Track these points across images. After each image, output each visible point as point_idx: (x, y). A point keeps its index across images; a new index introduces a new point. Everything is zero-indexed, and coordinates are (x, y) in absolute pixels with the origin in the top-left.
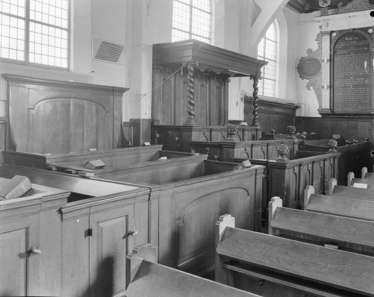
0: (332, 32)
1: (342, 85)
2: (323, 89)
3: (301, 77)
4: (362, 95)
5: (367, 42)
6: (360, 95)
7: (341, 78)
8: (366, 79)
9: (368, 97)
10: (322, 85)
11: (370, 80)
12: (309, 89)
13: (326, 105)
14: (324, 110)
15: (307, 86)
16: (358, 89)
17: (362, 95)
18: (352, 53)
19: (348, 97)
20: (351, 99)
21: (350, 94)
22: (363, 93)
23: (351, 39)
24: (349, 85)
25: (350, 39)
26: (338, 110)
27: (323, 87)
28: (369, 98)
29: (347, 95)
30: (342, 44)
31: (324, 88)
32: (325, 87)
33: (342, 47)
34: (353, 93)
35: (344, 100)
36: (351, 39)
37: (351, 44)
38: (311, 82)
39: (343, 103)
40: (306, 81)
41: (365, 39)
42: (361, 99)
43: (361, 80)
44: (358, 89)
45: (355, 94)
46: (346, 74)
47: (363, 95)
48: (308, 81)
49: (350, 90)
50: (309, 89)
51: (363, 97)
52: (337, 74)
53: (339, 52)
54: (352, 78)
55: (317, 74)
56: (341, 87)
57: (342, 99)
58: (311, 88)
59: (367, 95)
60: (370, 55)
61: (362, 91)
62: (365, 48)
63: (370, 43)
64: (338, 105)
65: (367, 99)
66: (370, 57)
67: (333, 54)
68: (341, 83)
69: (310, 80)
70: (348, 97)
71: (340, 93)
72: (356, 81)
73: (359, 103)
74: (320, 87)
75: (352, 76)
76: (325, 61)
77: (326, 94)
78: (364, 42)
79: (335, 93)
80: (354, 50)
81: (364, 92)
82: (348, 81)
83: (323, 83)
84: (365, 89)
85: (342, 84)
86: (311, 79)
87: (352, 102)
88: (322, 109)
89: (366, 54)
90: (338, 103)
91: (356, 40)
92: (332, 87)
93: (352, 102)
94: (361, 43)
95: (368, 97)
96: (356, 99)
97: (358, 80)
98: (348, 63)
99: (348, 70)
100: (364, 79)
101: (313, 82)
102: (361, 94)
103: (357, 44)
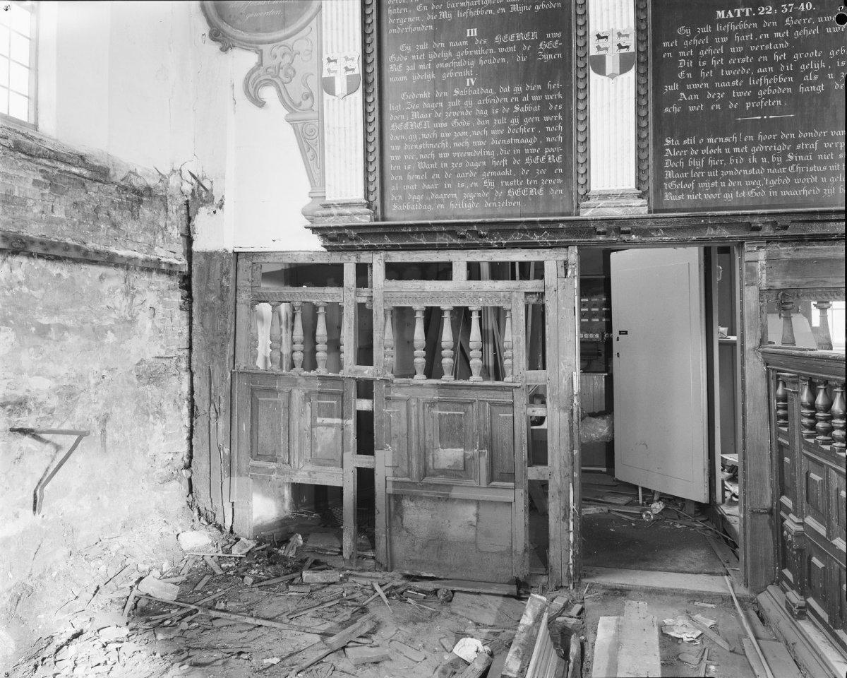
1: (421, 72)
2: (326, 96)
3: (216, 35)
4: (526, 121)
6: (515, 121)
7: (418, 38)
8: (542, 37)
9: (554, 134)
10: (325, 74)
11: (567, 40)
12: (260, 103)
13: (346, 184)
14: (334, 211)
15: (247, 79)
16: (508, 89)
19: (457, 135)
20: (471, 149)
21: (467, 118)
22: (530, 114)
24: (457, 69)
26: (405, 209)
27: (328, 86)
28: (560, 138)
29: (450, 129)
31: (332, 92)
32: (340, 85)
34: (479, 112)
35: (437, 151)
38: (268, 61)
39: (432, 171)
40: (243, 60)
42: (522, 147)
43: (519, 44)
44: (508, 89)
45: (490, 117)
46: (444, 15)
47: (530, 125)
48: (251, 59)
49: (464, 98)
50: (260, 103)
51: (529, 135)
52: (395, 16)
54: (472, 32)
55: (300, 16)
56: (421, 86)
57: (423, 151)
58: (269, 94)
59: (554, 123)
61: (526, 99)
64: (405, 182)
65: (551, 145)
68: (418, 62)
69: (260, 53)
70: (457, 135)
71: (415, 115)
72: (495, 46)
73: (510, 165)
74: (314, 84)
75: (471, 22)
77: (344, 116)
79: (389, 117)
82: (454, 50)
83: (329, 60)
84: (540, 93)
85: (422, 67)
86: (266, 48)
87: (477, 165)
88: (327, 206)
90: (404, 173)
92: (373, 82)
93: (477, 165)
95: (554, 134)
96: (496, 149)
97: (504, 45)
100: (535, 35)
101: (275, 62)
102: (522, 116)
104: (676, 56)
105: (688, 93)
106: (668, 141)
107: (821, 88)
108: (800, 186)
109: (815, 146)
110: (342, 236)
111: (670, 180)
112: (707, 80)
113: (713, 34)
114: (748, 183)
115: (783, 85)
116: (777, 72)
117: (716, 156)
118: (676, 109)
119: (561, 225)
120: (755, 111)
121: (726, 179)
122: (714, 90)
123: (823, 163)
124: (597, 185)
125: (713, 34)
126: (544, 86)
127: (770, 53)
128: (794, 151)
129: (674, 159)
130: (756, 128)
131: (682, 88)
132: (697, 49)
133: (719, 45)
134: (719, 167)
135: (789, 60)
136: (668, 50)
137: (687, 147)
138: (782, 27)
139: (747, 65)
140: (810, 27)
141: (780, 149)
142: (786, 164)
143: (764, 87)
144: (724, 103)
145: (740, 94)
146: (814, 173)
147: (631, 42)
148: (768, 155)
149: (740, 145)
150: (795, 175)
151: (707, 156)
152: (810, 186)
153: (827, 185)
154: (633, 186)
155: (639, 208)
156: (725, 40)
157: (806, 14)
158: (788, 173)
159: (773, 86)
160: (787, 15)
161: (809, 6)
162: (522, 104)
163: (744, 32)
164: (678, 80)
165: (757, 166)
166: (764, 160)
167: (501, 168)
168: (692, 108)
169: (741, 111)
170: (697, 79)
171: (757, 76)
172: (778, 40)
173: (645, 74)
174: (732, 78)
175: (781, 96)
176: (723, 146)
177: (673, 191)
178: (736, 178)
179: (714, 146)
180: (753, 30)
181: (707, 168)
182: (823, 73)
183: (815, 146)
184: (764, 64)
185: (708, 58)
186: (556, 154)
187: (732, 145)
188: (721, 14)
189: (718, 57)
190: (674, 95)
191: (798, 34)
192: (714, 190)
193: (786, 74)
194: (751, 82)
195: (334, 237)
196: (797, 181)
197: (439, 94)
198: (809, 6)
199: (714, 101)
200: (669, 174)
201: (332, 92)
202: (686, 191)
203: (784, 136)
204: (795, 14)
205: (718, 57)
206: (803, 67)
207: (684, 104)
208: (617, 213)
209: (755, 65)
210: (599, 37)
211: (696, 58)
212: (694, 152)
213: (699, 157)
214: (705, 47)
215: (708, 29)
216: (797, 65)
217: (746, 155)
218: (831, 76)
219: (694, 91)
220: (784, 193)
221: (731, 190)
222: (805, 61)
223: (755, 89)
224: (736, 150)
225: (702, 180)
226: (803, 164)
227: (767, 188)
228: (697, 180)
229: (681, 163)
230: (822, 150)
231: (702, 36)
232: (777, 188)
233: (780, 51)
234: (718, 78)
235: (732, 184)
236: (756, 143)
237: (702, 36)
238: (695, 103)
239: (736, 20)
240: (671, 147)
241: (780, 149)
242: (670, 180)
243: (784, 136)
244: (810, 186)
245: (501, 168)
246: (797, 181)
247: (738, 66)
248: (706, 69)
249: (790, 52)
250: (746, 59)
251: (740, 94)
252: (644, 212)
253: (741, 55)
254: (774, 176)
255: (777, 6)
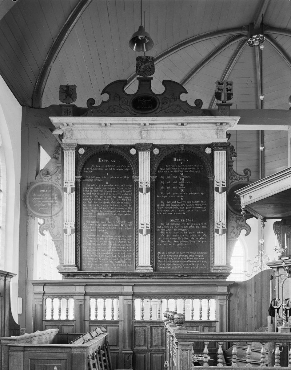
0: (79, 146)
1: (93, 229)
2: (65, 234)
4: (122, 245)
5: (128, 168)
10: (64, 228)
12: (43, 235)
17: (122, 245)
18: (107, 183)
23: (107, 161)
24: (103, 229)
25: (104, 161)
30: (93, 168)
31: (66, 233)
32: (69, 231)
33: (93, 171)
36: (107, 161)
37: (106, 168)
41: (126, 163)
47: (123, 246)
50: (43, 235)
52: (85, 212)
53: (88, 179)
54: (107, 219)
60: (133, 187)
62: (125, 177)
63: (133, 169)
65: (128, 252)
66: (133, 190)
67: (81, 182)
68: (92, 226)
69: (44, 220)
71: (91, 241)
72: (114, 224)
74: (61, 231)
76: (69, 190)
78: (124, 168)
80: (111, 178)
81: (124, 241)
83: (66, 224)
84: (126, 238)
86: (46, 219)
89: (127, 186)
91: (113, 163)
92: (78, 231)
94: (120, 168)
95: (129, 249)
98: (101, 197)
99: (102, 207)
100: (124, 222)
103: (114, 169)
104: (161, 231)
105: (163, 240)
106: (158, 253)
107: (195, 241)
108: (190, 266)
109: (193, 256)
110: (68, 275)
111: (159, 263)
112: (168, 237)
113: (170, 226)
114: (178, 265)
115: (186, 240)
116: (185, 236)
117: (170, 257)
118: (161, 244)
119: (131, 274)
120: (180, 246)
121: (173, 263)
122: (170, 240)
123: (195, 260)
124: (140, 264)
125: (170, 226)
126: (127, 236)
127: (183, 232)
128: (188, 256)
129: (160, 257)
130: (180, 250)
131: (162, 239)
132: (166, 229)
133: (171, 228)
134: (171, 260)
135: (188, 234)
136: (159, 228)
137: (163, 254)
138: (186, 225)
139: (178, 234)
140: (193, 226)
141: (186, 256)
142: (187, 260)
143: (182, 240)
144: (172, 243)
145: (176, 241)
146: (193, 263)
147: (149, 226)
148: (183, 258)
149: (177, 255)
150: (188, 263)
151: (168, 257)
152: (192, 266)
153: (196, 266)
154: (150, 264)
155: (151, 270)
156: (172, 227)
157: (192, 222)
158: (187, 263)
159: (184, 240)
160: (187, 222)
161: (192, 220)
162: (121, 241)
163: (177, 226)
164: (161, 237)
165: (180, 260)
166: (182, 259)
167: (115, 258)
168: (164, 244)
169: (176, 246)
170: (166, 237)
171: (180, 237)
172: (184, 229)
173: (153, 235)
174: (174, 237)
175: (186, 243)
176: (172, 255)
177: (160, 266)
178: (175, 263)
179: (169, 255)
180: (179, 225)
181: (168, 260)
182: (195, 238)
183: (193, 256)
184: (182, 234)
185: (168, 231)
186: (130, 255)
187: (174, 255)
188: (172, 220)
189: (171, 231)
190: (160, 241)
191: (190, 227)
192: (169, 266)
193: (187, 237)
194: (179, 239)
195: (67, 275)
196: (189, 265)
197: (97, 236)
198: (192, 220)
199: (170, 243)
200: (159, 261)
201: (66, 233)
202: (163, 266)
203: (186, 253)
204: (189, 222)
205: (171, 231)
206: (191, 236)
207: (163, 243)
208: (146, 271)
209: (180, 234)
210: (141, 224)
211: (165, 231)
212: (165, 256)
213: (166, 257)
214: (168, 229)
215: (168, 224)
216: (189, 235)
217: (178, 257)
218: (197, 239)
219: (165, 240)
220: (186, 267)
221: (174, 266)
222: (191, 234)
223: (180, 241)
224: (175, 256)
225: (167, 263)
226: (191, 260)
227: (182, 266)
228: (166, 263)
229: (162, 259)
230: (195, 257)
231: (167, 226)
232: (185, 266)
233: (186, 231)
234: (171, 237)
235: (174, 264)
236: (180, 254)
237: (167, 226)
238: (165, 243)
239: (175, 222)
240: (159, 254)
241: (186, 256)
242: (159, 263)
243: (186, 253)
244: (192, 266)
245: (115, 258)
246: (189, 265)
247: (175, 234)
248: (168, 234)
249: (188, 232)
250: (178, 233)
251: (176, 241)
252: (152, 271)
253: (177, 231)
254: (184, 263)
255: (185, 220)
